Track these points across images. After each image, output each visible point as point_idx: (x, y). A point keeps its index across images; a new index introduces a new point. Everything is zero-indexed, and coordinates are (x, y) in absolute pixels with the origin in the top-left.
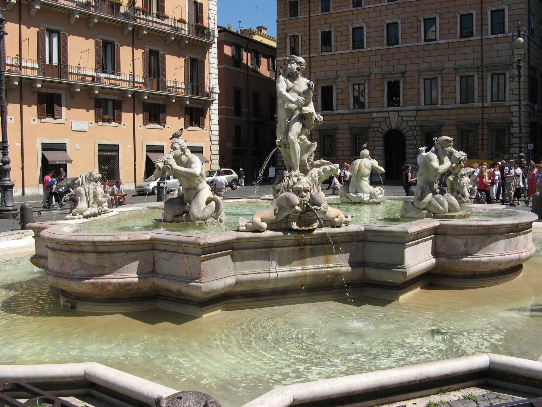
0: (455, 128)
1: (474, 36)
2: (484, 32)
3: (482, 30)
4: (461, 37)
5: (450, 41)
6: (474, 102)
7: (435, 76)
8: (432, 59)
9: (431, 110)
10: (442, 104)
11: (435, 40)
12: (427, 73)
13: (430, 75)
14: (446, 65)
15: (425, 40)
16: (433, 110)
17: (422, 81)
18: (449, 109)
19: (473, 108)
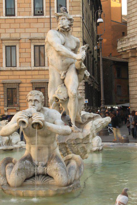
0: (31, 85)
1: (45, 14)
2: (51, 12)
3: (50, 11)
4: (35, 15)
5: (26, 17)
6: (44, 66)
7: (14, 44)
8: (12, 31)
9: (11, 70)
10: (20, 66)
11: (14, 15)
12: (8, 41)
13: (10, 43)
14: (23, 36)
15: (6, 15)
16: (13, 71)
17: (4, 48)
18: (26, 70)
19: (44, 70)
